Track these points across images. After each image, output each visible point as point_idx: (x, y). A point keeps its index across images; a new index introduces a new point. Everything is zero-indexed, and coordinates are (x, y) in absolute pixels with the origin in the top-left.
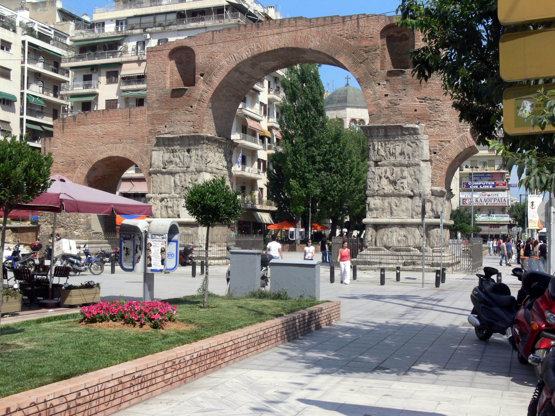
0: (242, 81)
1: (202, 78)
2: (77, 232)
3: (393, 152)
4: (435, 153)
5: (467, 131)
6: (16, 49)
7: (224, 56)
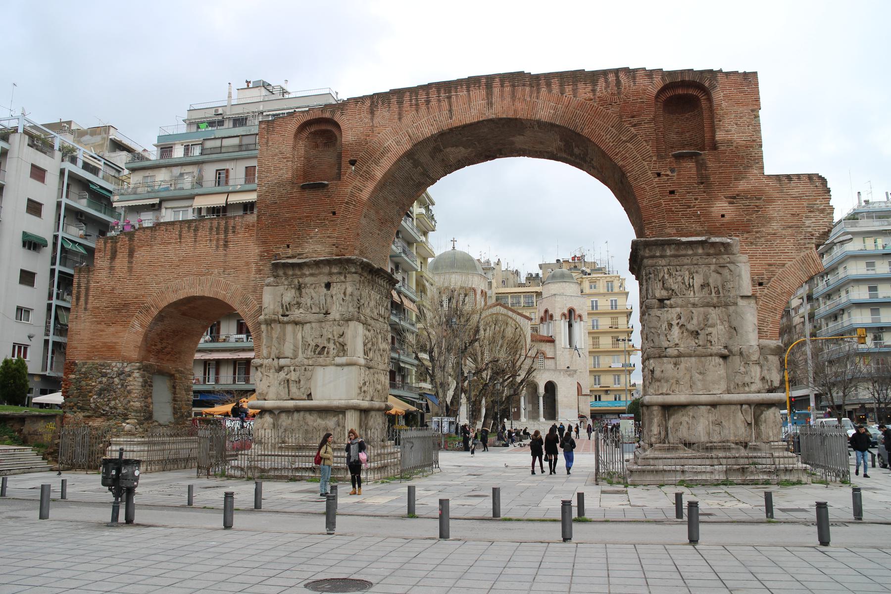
0: (412, 179)
2: (128, 423)
3: (689, 284)
4: (760, 284)
5: (811, 248)
6: (52, 178)
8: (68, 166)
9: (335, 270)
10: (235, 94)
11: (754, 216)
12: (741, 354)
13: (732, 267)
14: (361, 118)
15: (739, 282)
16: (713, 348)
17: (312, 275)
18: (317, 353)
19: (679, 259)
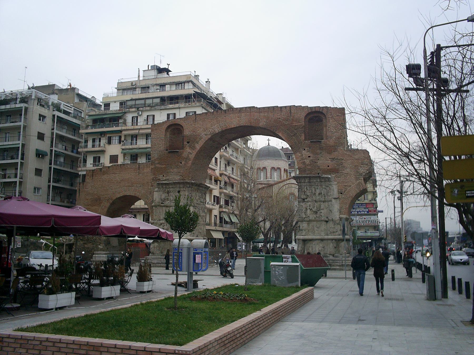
2: (101, 246)
4: (341, 193)
5: (361, 179)
6: (49, 120)
8: (57, 113)
9: (181, 186)
10: (141, 75)
11: (340, 166)
13: (330, 187)
14: (191, 124)
16: (322, 218)
17: (172, 188)
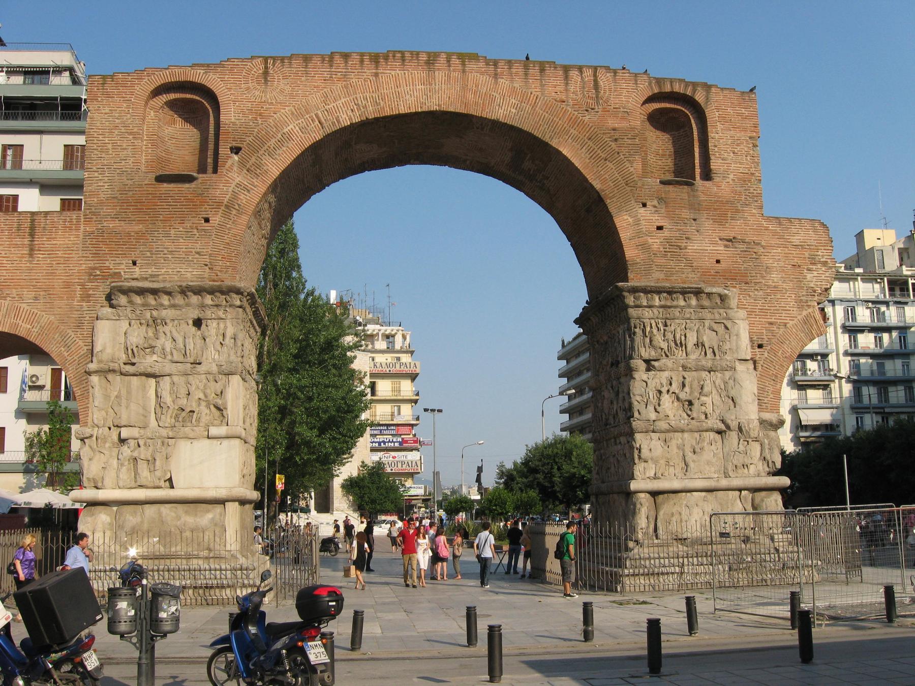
1: (236, 158)
4: (760, 346)
7: (293, 114)
9: (208, 300)
12: (740, 429)
14: (248, 88)
15: (737, 342)
18: (180, 419)
19: (670, 310)
